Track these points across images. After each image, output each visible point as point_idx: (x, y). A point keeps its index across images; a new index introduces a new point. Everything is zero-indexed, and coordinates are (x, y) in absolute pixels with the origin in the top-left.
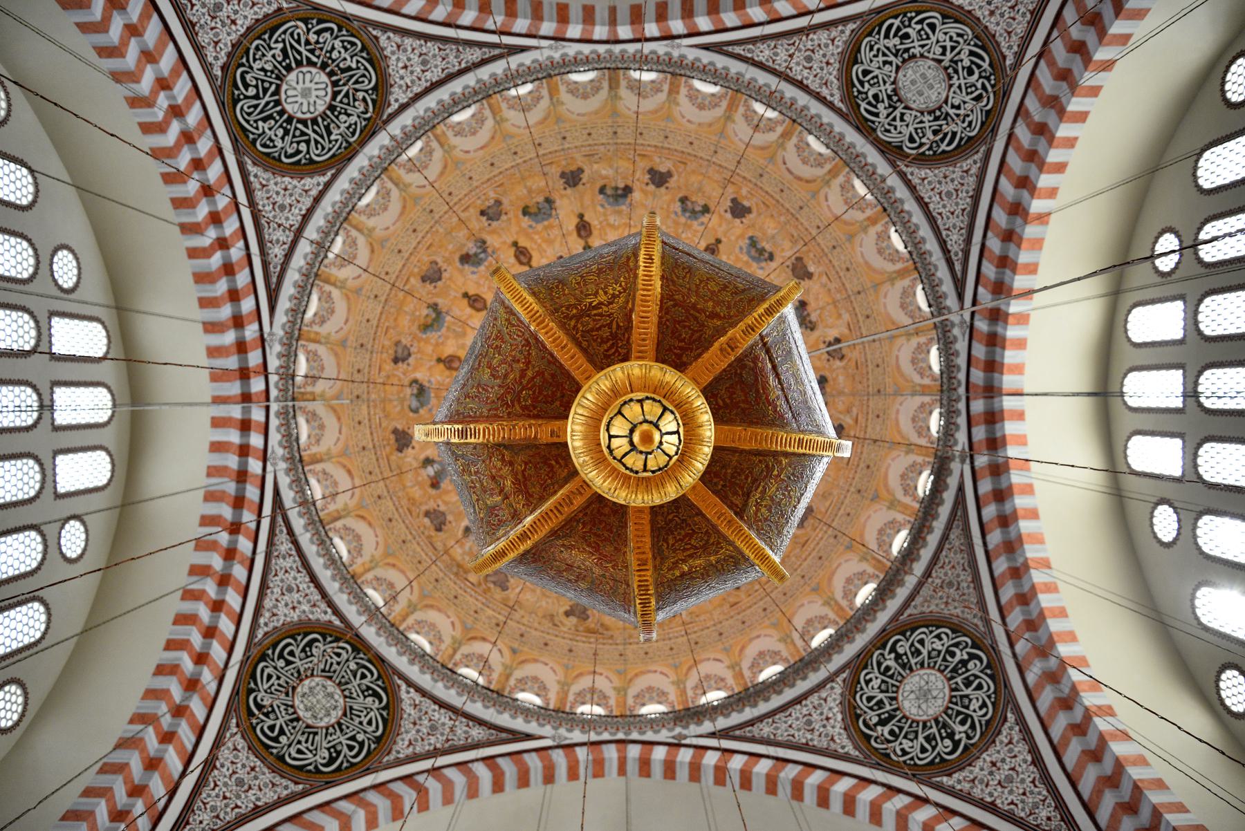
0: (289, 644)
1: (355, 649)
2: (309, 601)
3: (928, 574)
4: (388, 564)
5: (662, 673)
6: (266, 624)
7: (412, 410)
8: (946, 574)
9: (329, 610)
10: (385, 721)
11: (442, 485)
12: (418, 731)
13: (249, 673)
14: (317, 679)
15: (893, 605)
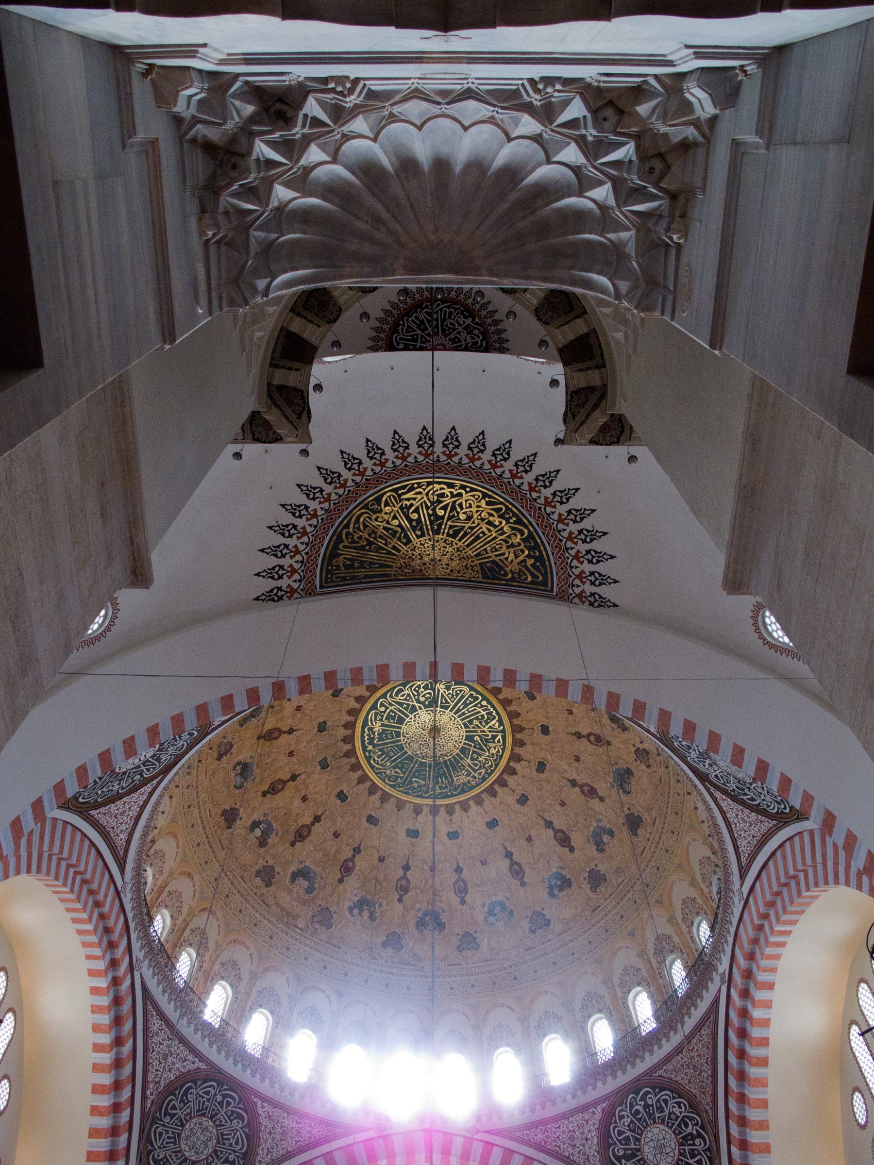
0: (172, 1100)
1: (220, 1083)
2: (180, 1059)
3: (678, 1050)
4: (230, 942)
5: (463, 1013)
6: (152, 1094)
7: (237, 788)
8: (692, 1058)
9: (196, 1059)
10: (248, 1136)
11: (269, 841)
12: (273, 1139)
13: (145, 1139)
14: (194, 1120)
15: (649, 1061)
